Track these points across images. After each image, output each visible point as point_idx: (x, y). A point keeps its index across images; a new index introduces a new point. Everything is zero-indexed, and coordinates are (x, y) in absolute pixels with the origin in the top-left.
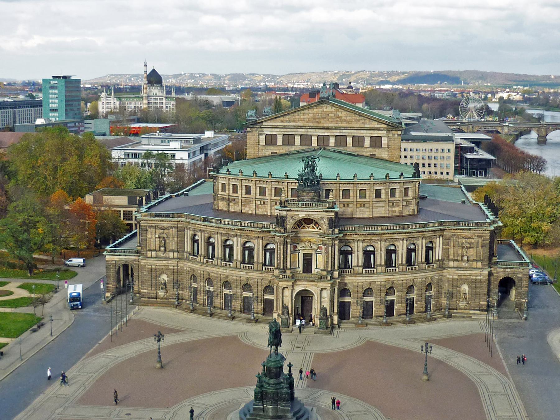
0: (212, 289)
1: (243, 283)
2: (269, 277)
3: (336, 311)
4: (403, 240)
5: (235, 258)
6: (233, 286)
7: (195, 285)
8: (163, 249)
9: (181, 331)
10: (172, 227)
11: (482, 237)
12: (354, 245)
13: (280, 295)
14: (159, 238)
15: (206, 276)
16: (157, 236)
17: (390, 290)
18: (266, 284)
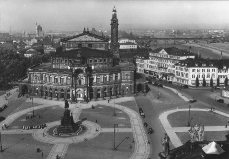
0: (52, 91)
1: (61, 89)
2: (68, 87)
3: (89, 96)
4: (108, 74)
5: (58, 82)
6: (58, 90)
7: (46, 90)
8: (36, 80)
9: (41, 105)
10: (39, 73)
11: (131, 72)
12: (94, 77)
13: (72, 92)
14: (35, 77)
15: (50, 88)
16: (34, 76)
17: (105, 89)
18: (68, 89)
